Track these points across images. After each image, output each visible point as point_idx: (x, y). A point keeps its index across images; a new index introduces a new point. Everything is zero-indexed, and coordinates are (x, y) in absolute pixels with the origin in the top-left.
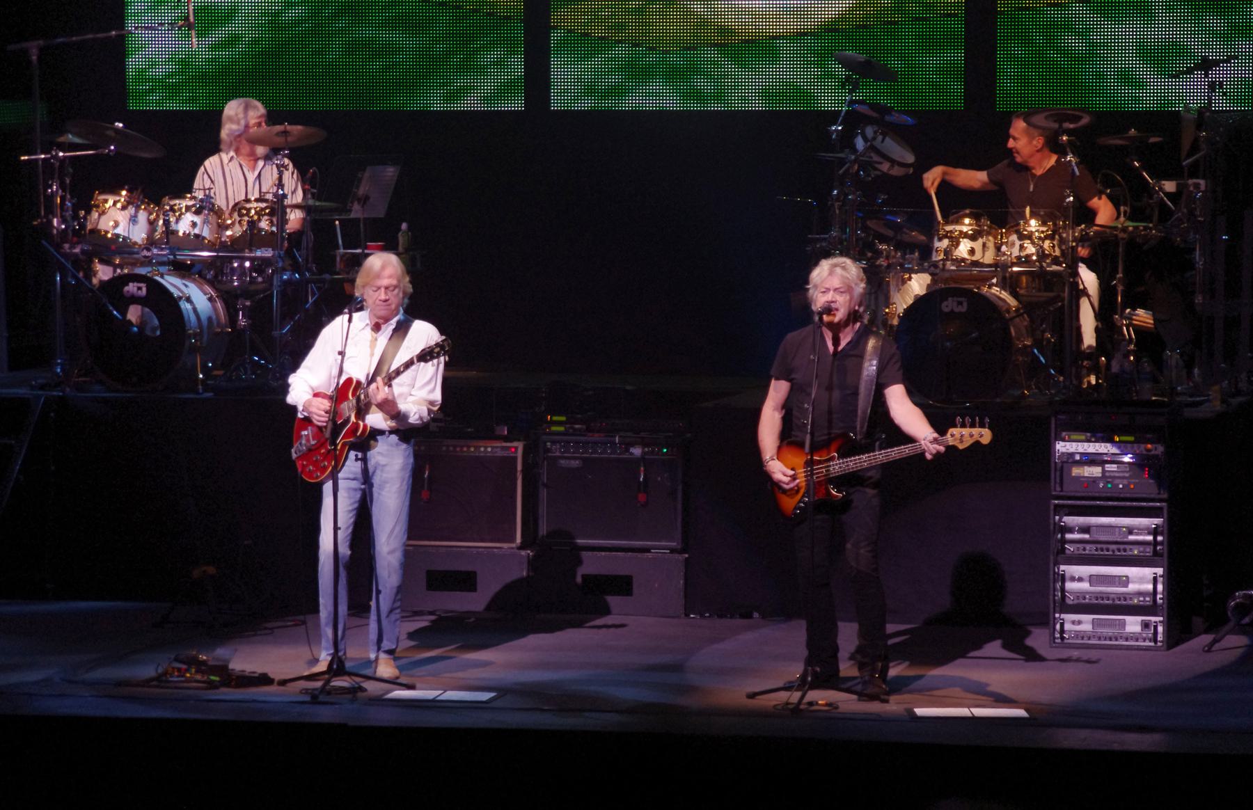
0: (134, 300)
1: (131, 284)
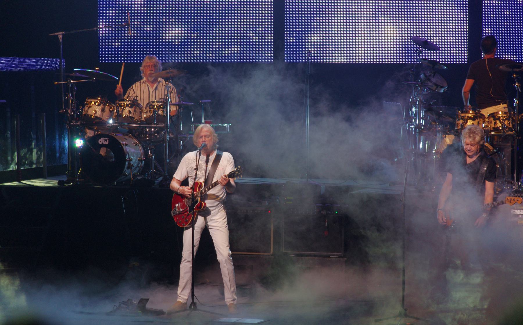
0: (103, 145)
1: (102, 138)
